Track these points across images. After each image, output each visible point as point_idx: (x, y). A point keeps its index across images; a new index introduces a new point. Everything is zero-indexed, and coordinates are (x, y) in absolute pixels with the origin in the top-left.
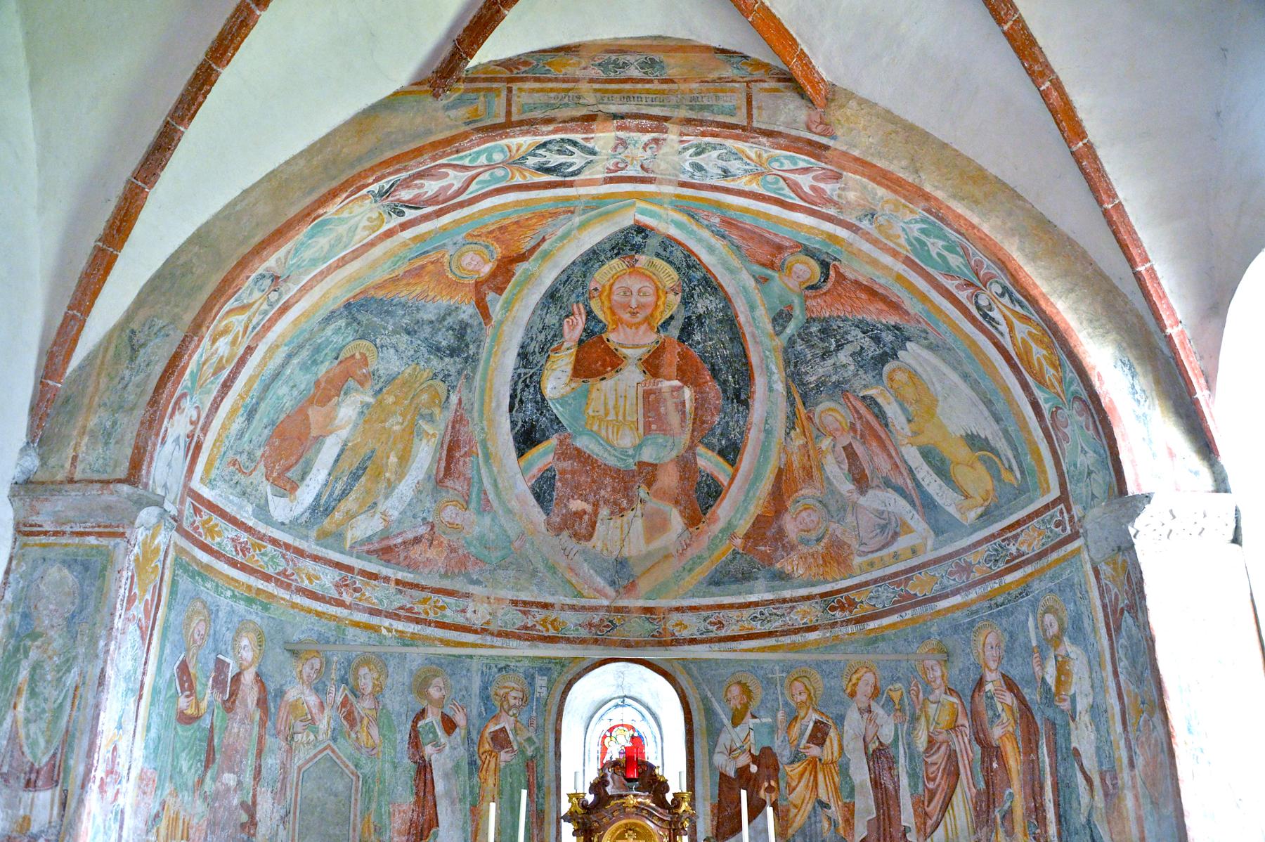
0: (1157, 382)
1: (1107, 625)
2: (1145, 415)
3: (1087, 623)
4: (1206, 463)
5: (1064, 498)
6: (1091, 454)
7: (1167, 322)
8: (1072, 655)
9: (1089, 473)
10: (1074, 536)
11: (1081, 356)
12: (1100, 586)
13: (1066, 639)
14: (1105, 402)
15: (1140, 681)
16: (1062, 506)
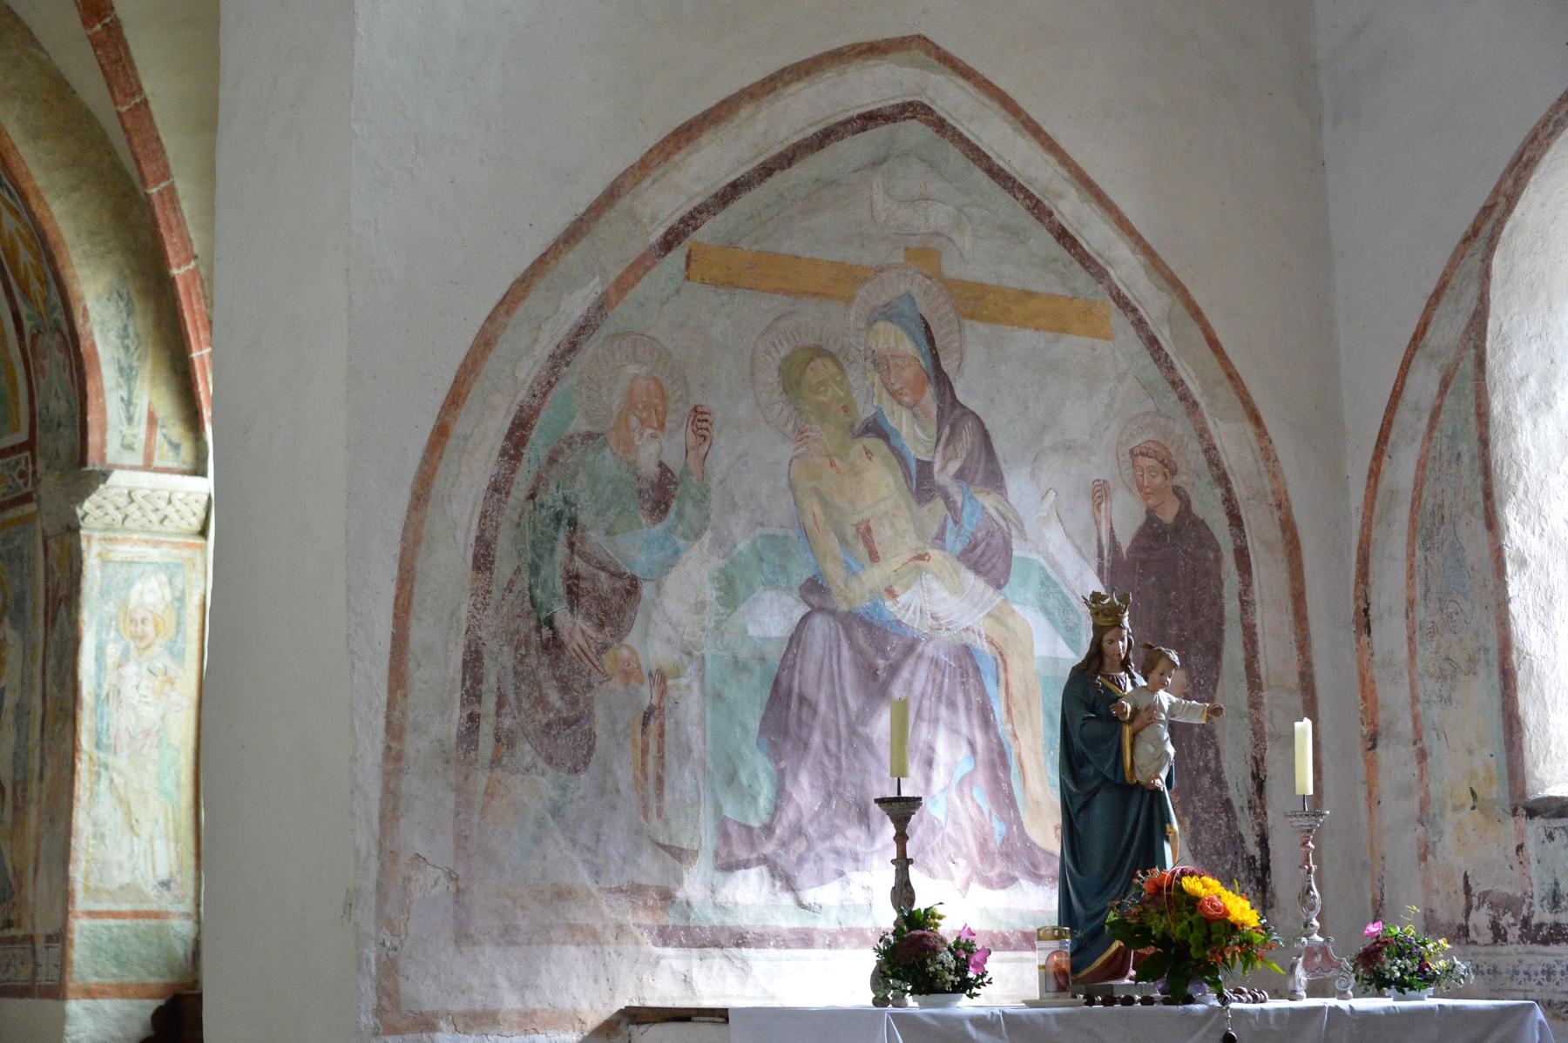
0: (158, 325)
1: (46, 613)
2: (131, 368)
3: (28, 605)
4: (191, 435)
5: (29, 445)
6: (63, 403)
7: (172, 261)
8: (10, 642)
9: (59, 425)
10: (27, 499)
11: (68, 281)
12: (46, 566)
13: (6, 619)
14: (84, 345)
15: (62, 685)
16: (27, 454)
